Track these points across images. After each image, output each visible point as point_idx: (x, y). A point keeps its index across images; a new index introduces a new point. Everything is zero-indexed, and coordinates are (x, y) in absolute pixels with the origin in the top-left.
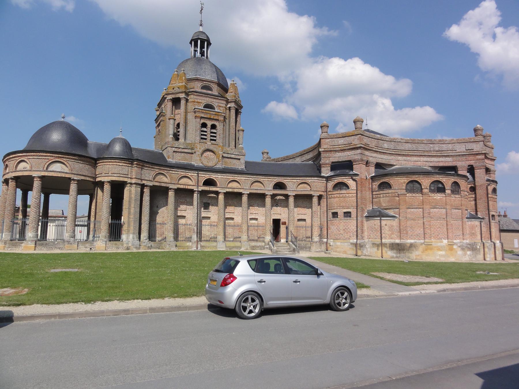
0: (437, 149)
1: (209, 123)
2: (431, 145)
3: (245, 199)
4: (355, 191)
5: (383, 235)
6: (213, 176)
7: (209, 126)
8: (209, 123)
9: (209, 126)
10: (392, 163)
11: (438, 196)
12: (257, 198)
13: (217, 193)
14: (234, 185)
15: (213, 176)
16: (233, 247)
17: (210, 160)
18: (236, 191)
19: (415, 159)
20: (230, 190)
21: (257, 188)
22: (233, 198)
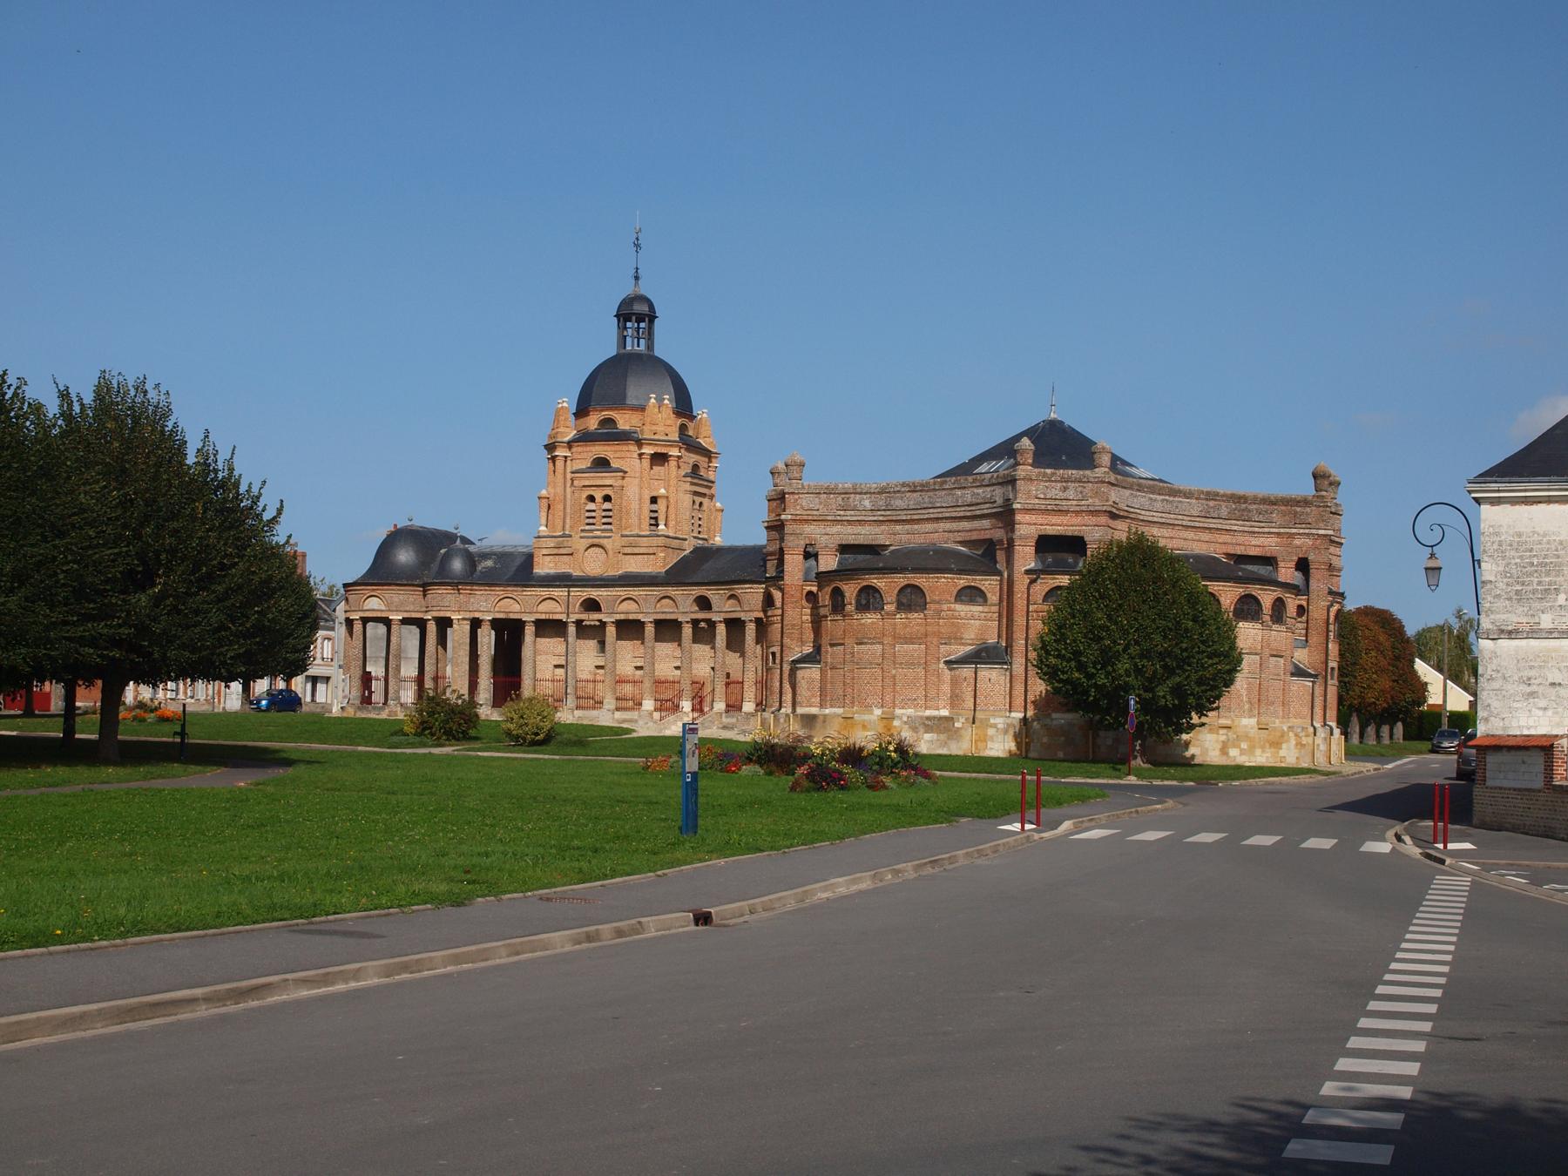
0: (969, 499)
1: (598, 496)
2: (959, 493)
3: (650, 630)
4: (779, 612)
5: (799, 699)
6: (594, 593)
7: (599, 498)
8: (598, 496)
9: (599, 498)
10: (882, 540)
11: (870, 618)
12: (668, 629)
13: (603, 624)
14: (626, 606)
15: (594, 593)
16: (624, 721)
17: (593, 564)
18: (631, 617)
19: (929, 527)
20: (622, 617)
21: (666, 610)
22: (631, 629)
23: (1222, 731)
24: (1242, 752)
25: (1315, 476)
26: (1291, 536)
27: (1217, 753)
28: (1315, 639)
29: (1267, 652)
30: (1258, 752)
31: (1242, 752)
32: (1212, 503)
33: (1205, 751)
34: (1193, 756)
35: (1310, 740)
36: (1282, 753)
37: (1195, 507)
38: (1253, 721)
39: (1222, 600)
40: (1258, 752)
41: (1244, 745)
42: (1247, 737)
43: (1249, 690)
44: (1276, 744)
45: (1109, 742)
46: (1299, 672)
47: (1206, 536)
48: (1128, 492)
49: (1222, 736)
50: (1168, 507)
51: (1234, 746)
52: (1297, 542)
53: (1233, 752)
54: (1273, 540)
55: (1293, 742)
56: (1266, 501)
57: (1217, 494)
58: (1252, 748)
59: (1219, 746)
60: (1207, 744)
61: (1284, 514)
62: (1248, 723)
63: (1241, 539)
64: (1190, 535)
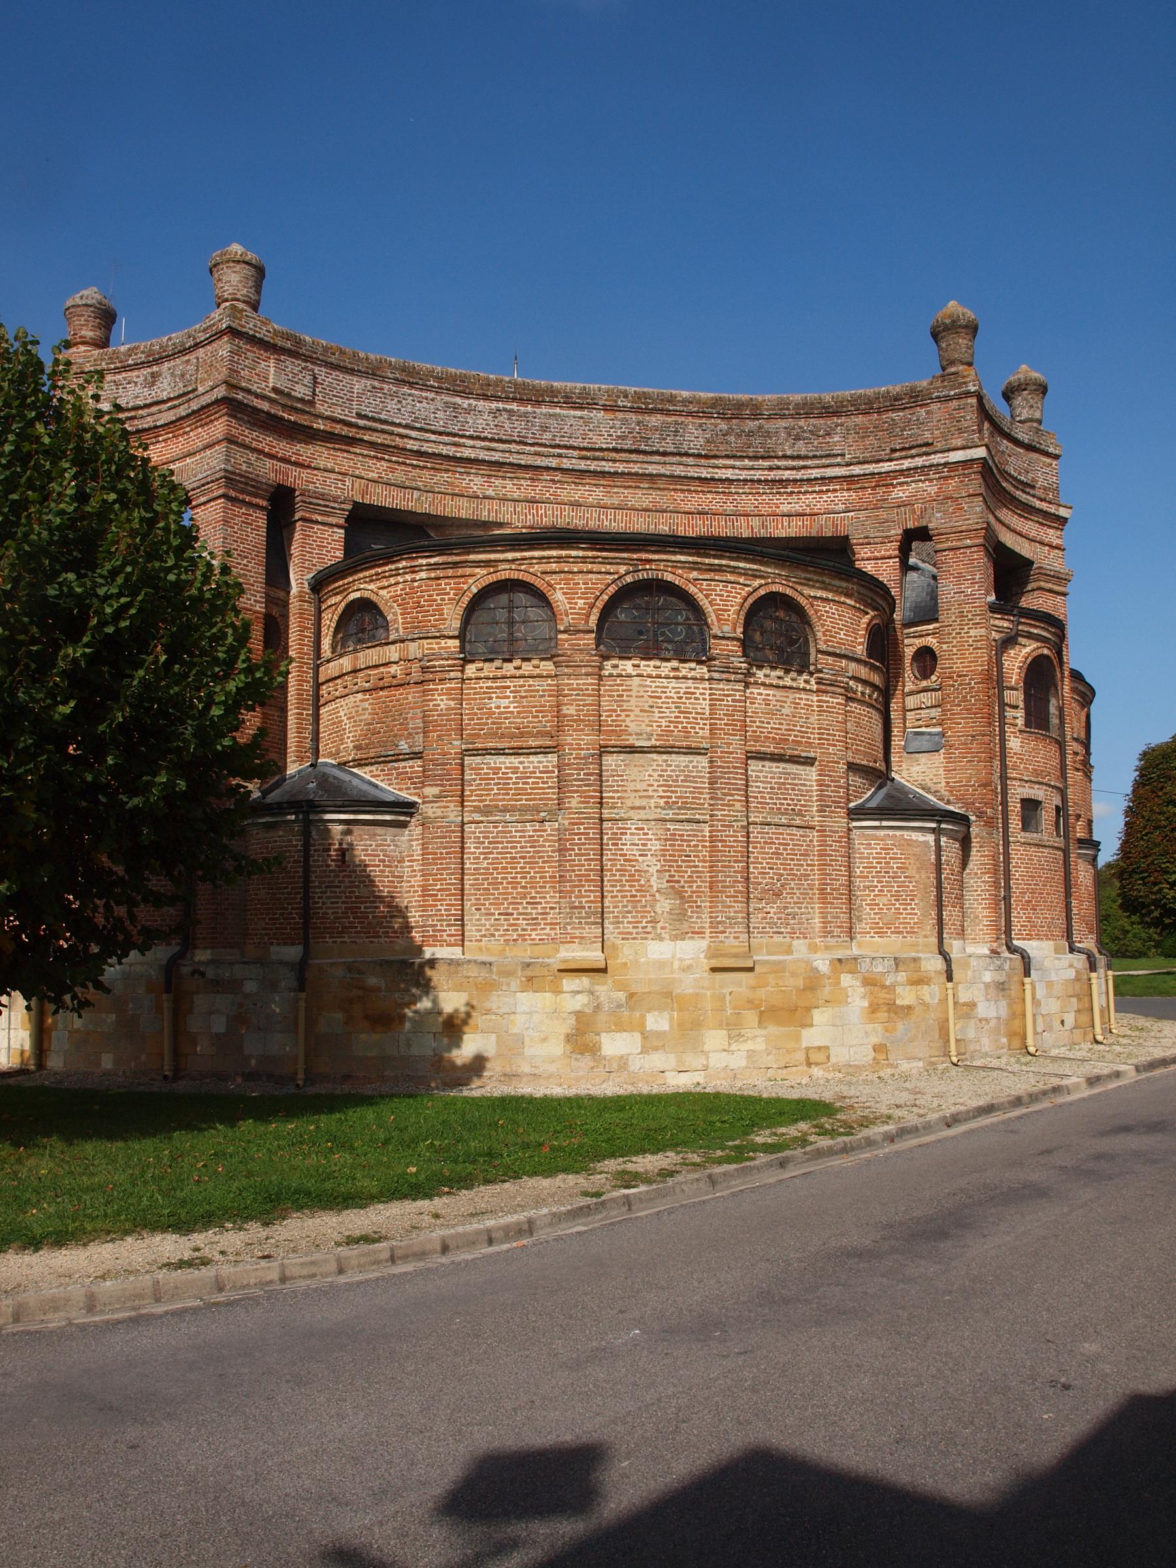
23: (570, 983)
24: (650, 1042)
25: (935, 336)
26: (884, 480)
27: (556, 1047)
28: (962, 727)
29: (736, 746)
30: (714, 1039)
31: (650, 1042)
32: (655, 420)
33: (513, 1045)
34: (478, 1064)
35: (931, 993)
36: (811, 1037)
37: (603, 429)
38: (693, 950)
39: (558, 597)
40: (714, 1039)
41: (658, 1022)
42: (667, 997)
43: (674, 856)
44: (790, 1013)
45: (219, 1025)
46: (902, 808)
47: (641, 497)
48: (359, 385)
49: (574, 996)
50: (517, 428)
51: (620, 1027)
52: (900, 493)
53: (614, 1045)
54: (841, 497)
55: (858, 1000)
56: (806, 410)
57: (672, 399)
58: (689, 1031)
59: (566, 1026)
60: (518, 1024)
61: (863, 433)
62: (672, 956)
63: (748, 502)
64: (594, 493)
